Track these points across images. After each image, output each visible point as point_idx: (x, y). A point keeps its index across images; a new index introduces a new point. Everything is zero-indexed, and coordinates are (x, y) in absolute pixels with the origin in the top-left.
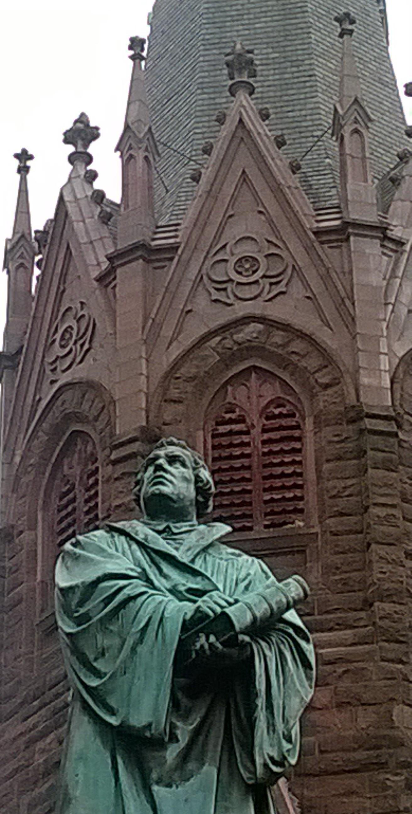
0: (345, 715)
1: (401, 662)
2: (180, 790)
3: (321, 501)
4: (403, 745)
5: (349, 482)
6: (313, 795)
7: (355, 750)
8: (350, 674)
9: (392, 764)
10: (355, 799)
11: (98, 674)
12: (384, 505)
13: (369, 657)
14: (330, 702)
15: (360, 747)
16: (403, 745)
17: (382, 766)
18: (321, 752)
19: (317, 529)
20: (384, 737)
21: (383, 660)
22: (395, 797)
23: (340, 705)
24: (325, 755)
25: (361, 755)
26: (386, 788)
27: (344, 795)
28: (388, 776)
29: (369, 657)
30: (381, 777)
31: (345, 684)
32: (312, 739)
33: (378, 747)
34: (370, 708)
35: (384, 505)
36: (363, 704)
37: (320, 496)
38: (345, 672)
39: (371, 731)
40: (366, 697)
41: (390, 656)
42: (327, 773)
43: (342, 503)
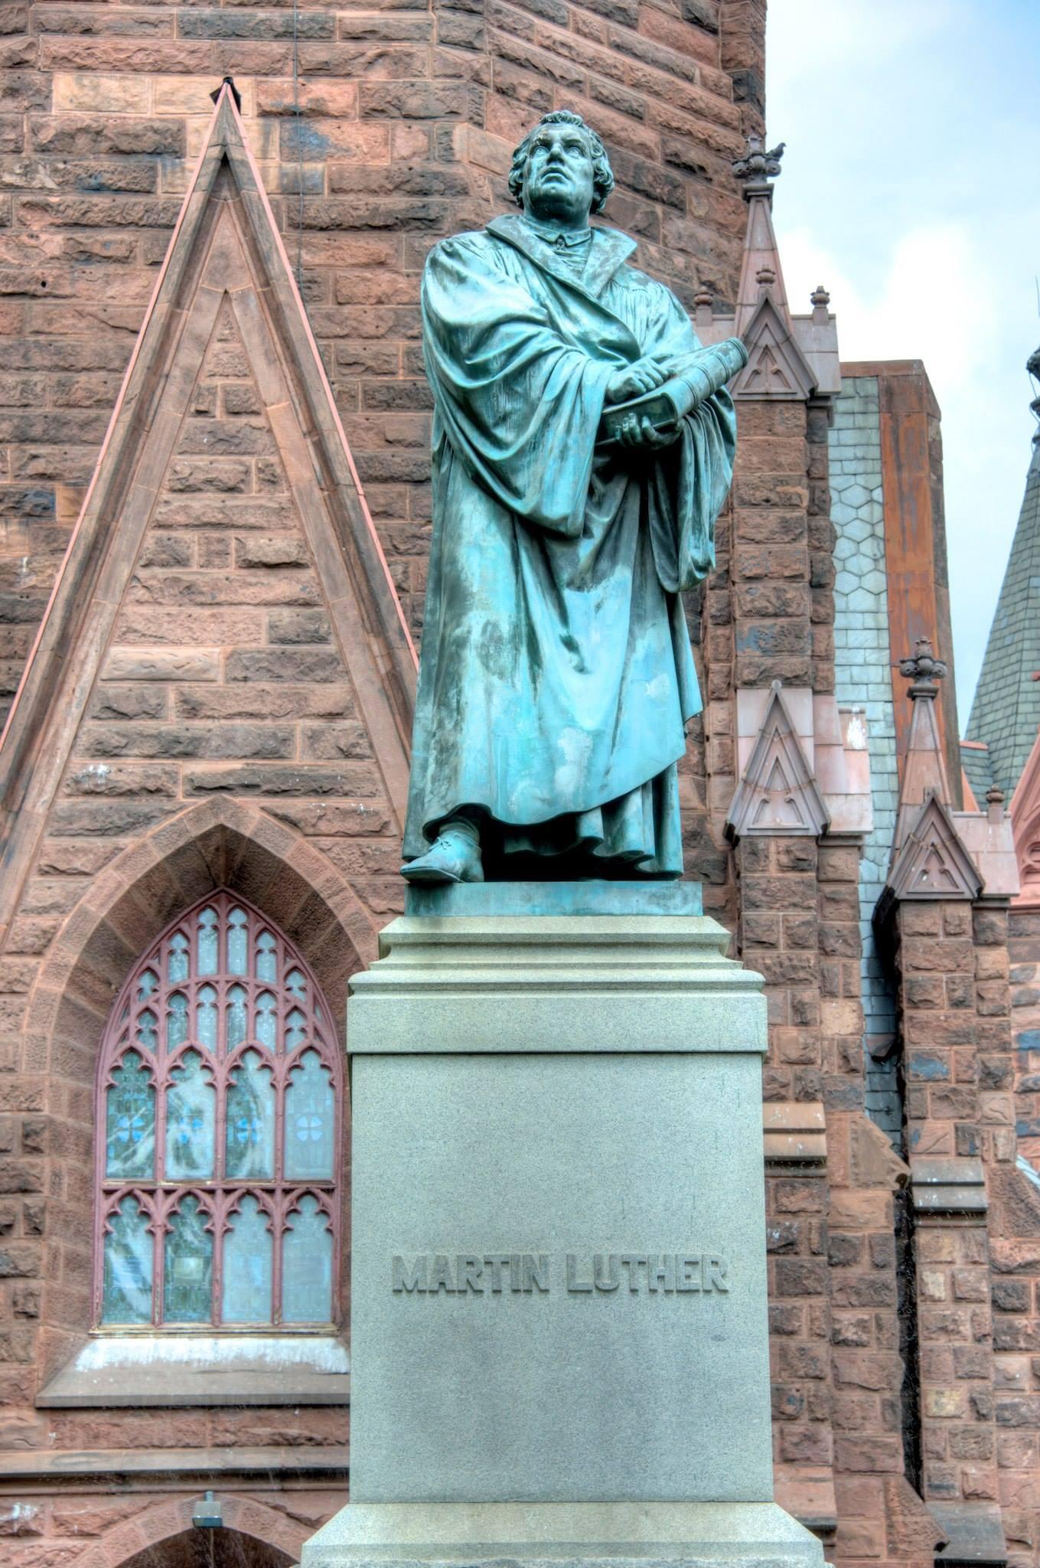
0: (375, 130)
1: (471, 47)
2: (595, 594)
4: (467, 193)
6: (317, 261)
7: (388, 192)
8: (387, 61)
10: (384, 276)
11: (498, 443)
13: (420, 34)
14: (352, 107)
15: (397, 188)
16: (467, 193)
18: (333, 191)
20: (436, 175)
21: (442, 42)
23: (370, 114)
24: (341, 197)
25: (399, 203)
27: (366, 266)
29: (420, 34)
31: (378, 76)
32: (320, 166)
33: (425, 193)
34: (417, 126)
36: (407, 117)
38: (381, 55)
39: (416, 163)
40: (413, 103)
41: (457, 34)
42: (339, 227)
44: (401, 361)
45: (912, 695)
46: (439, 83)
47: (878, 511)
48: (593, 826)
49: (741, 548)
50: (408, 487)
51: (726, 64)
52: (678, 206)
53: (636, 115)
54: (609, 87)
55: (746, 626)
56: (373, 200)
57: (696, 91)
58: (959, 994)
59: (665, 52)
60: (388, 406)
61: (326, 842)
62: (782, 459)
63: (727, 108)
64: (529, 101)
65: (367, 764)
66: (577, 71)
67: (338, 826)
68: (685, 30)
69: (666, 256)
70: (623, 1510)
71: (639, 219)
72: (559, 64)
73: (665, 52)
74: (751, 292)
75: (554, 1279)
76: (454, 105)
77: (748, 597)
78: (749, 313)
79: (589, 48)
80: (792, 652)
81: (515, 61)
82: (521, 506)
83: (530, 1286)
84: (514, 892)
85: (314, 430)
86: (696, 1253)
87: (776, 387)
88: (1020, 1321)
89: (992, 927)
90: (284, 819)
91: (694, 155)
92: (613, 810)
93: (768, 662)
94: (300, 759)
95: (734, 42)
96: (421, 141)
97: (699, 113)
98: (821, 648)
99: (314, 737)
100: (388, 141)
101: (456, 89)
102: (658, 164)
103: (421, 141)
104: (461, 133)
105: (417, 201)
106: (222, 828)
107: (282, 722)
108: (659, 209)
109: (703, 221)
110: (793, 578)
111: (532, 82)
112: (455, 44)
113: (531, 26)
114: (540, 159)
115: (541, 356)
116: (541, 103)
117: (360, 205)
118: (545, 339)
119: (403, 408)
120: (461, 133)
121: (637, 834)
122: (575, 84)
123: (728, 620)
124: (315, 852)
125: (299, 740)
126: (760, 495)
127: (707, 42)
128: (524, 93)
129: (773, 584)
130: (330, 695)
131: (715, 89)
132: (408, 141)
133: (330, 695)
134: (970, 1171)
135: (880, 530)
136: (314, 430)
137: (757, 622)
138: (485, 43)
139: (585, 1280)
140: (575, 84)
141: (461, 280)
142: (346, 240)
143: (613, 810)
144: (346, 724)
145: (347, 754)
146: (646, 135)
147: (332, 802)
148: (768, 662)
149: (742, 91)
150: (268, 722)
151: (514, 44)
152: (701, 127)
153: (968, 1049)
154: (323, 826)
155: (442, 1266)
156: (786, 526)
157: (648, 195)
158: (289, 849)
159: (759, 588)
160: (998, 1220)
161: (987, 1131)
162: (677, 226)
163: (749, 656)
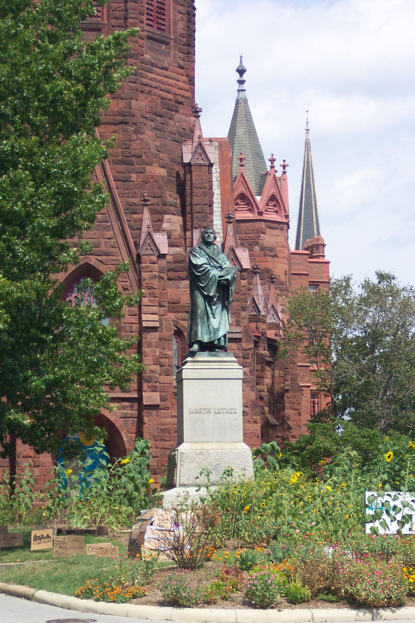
1: (135, 83)
2: (216, 306)
3: (108, 11)
5: (121, 5)
9: (130, 123)
11: (202, 283)
12: (133, 18)
15: (119, 115)
17: (126, 123)
18: (105, 115)
19: (106, 22)
20: (128, 112)
21: (129, 82)
22: (131, 135)
25: (120, 118)
26: (127, 131)
28: (129, 127)
30: (126, 127)
33: (125, 116)
34: (124, 101)
35: (133, 18)
37: (109, 7)
39: (123, 109)
40: (123, 96)
41: (133, 80)
42: (107, 124)
43: (117, 14)
44: (120, 154)
45: (228, 222)
46: (129, 91)
47: (218, 174)
48: (216, 342)
49: (194, 198)
50: (122, 182)
51: (187, 76)
52: (177, 112)
53: (169, 92)
54: (163, 87)
55: (195, 215)
56: (114, 117)
57: (181, 84)
58: (237, 291)
59: (175, 75)
60: (118, 164)
61: (108, 266)
62: (203, 178)
63: (187, 87)
64: (147, 93)
65: (118, 249)
66: (156, 84)
67: (111, 263)
68: (178, 69)
69: (175, 123)
70: (222, 444)
71: (169, 116)
72: (153, 83)
73: (175, 75)
74: (196, 139)
75: (212, 411)
76: (132, 96)
77: (196, 208)
78: (195, 144)
79: (159, 78)
80: (205, 221)
81: (144, 85)
82: (205, 293)
83: (209, 412)
84: (206, 353)
85: (106, 176)
86: (232, 408)
87: (202, 162)
88: (248, 360)
89: (244, 276)
90: (100, 261)
91: (181, 99)
92: (219, 340)
93: (200, 223)
94: (103, 248)
95: (189, 71)
96: (125, 104)
97: (181, 89)
98: (211, 220)
99: (106, 243)
100: (117, 104)
101: (132, 93)
102: (173, 103)
103: (125, 104)
104: (134, 102)
105: (123, 118)
106: (87, 263)
107: (99, 240)
108: (173, 113)
109: (182, 114)
110: (206, 204)
111: (147, 89)
112: (132, 82)
113: (147, 76)
114: (206, 235)
115: (209, 270)
116: (149, 93)
117: (111, 119)
118: (209, 268)
119: (121, 164)
120: (134, 102)
121: (222, 343)
122: (156, 88)
123: (191, 213)
124: (106, 268)
125: (103, 244)
126: (198, 186)
127: (182, 71)
128: (146, 91)
129: (201, 206)
130: (110, 234)
131: (185, 82)
132: (122, 104)
133: (110, 234)
134: (239, 330)
135: (219, 179)
136: (106, 176)
137: (197, 214)
138: (138, 82)
139: (217, 411)
140: (156, 88)
141: (196, 256)
142: (107, 126)
143: (219, 340)
144: (112, 240)
145: (113, 247)
146: (170, 96)
147: (110, 257)
148: (200, 223)
149: (190, 83)
150: (96, 240)
151: (144, 81)
152: (182, 92)
153: (238, 303)
154: (108, 263)
155: (196, 409)
156: (204, 193)
157: (171, 110)
158: (101, 267)
159: (198, 206)
160: (243, 340)
161: (242, 320)
162: (177, 116)
163: (195, 221)
